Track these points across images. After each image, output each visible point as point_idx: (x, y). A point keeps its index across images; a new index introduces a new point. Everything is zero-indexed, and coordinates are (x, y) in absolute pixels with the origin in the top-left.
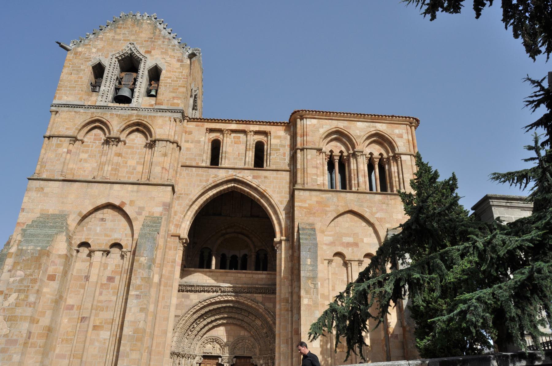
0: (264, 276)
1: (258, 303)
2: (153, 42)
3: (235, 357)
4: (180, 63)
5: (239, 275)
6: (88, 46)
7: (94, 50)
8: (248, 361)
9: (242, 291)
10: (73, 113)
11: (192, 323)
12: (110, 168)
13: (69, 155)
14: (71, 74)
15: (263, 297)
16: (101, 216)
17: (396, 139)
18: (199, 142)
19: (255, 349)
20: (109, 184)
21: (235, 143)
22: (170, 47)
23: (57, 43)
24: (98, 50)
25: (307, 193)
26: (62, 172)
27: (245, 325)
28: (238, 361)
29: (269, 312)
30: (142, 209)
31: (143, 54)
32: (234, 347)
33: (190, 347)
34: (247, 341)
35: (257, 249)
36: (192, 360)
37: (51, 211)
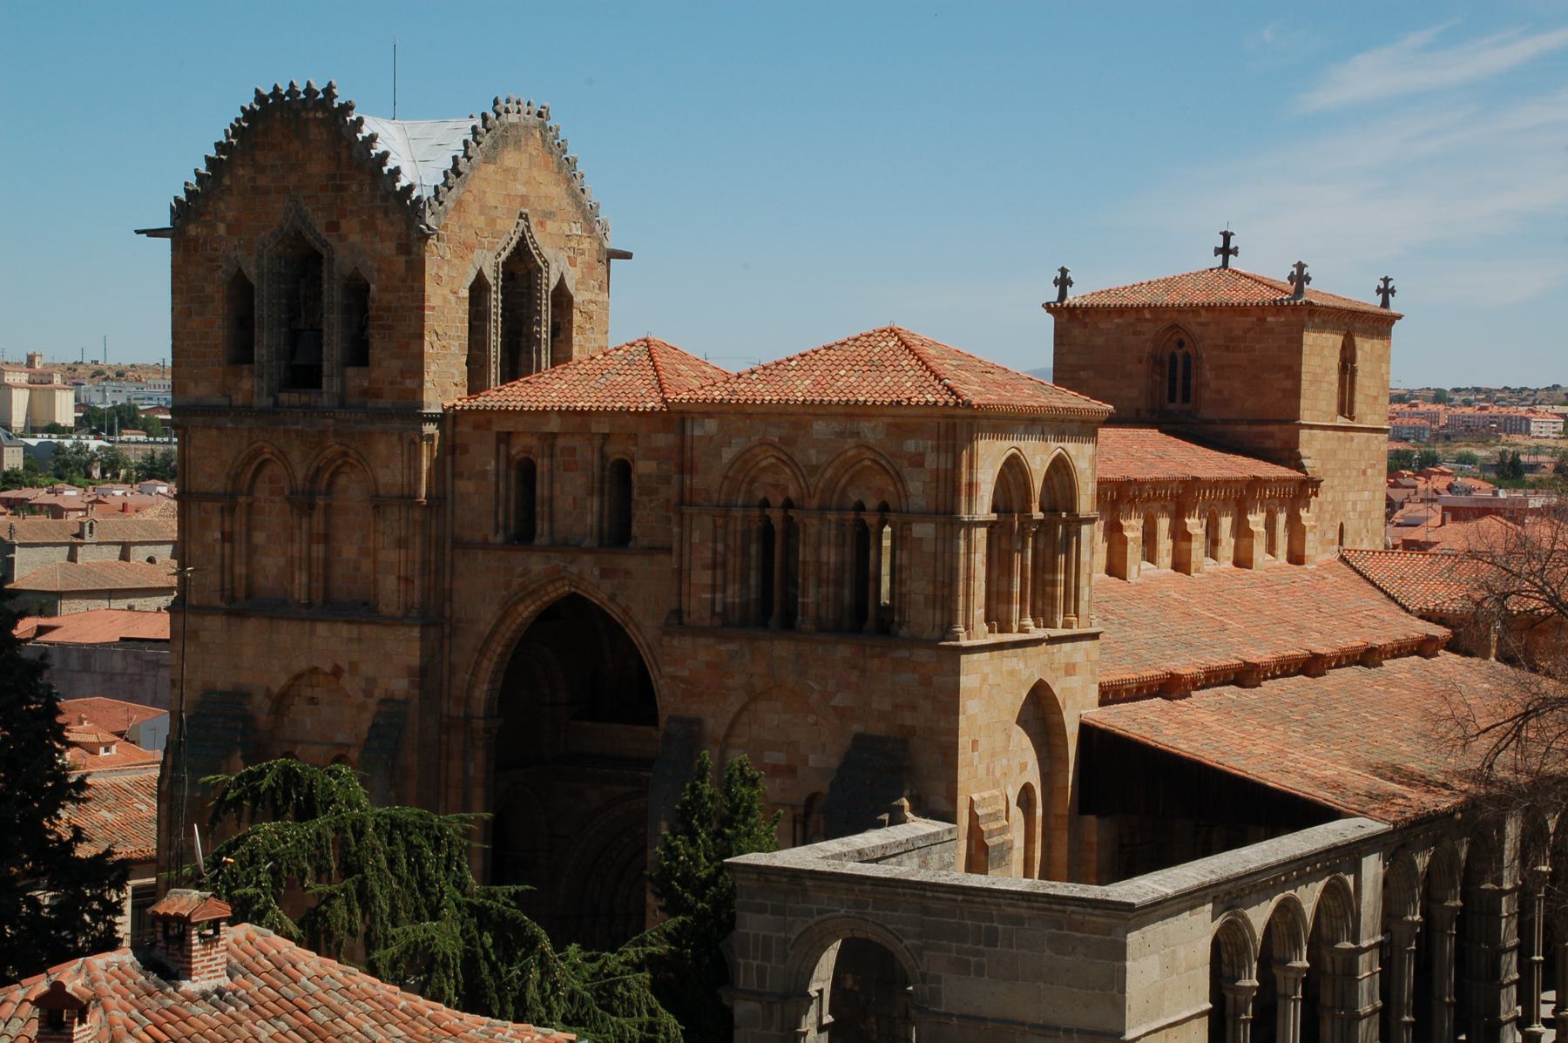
2: (340, 188)
4: (403, 258)
6: (208, 218)
7: (222, 229)
10: (214, 433)
12: (304, 579)
13: (227, 546)
14: (190, 315)
16: (308, 692)
17: (907, 471)
18: (483, 475)
20: (308, 623)
21: (566, 470)
22: (378, 202)
23: (138, 232)
24: (231, 229)
25: (687, 642)
26: (223, 589)
30: (371, 681)
31: (324, 235)
37: (220, 686)
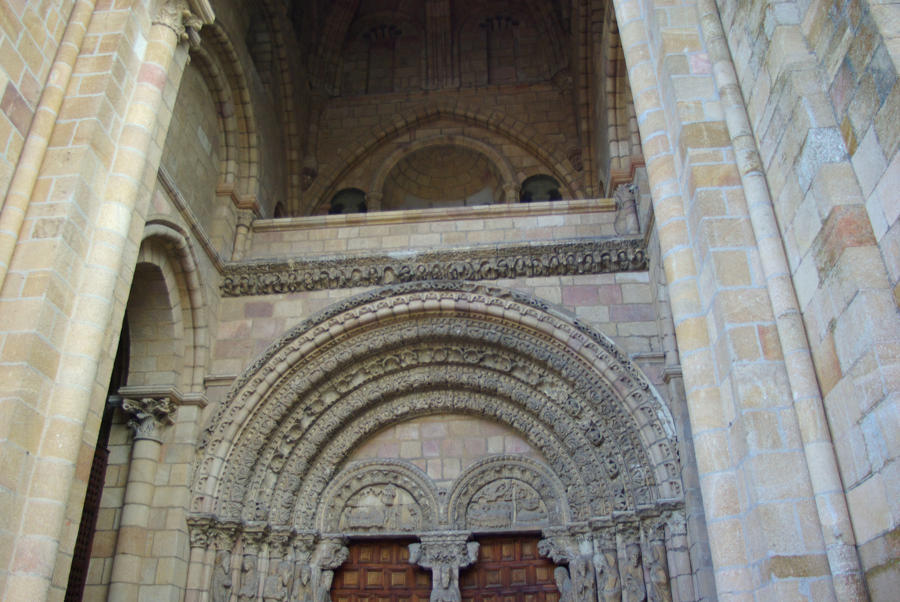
0: (558, 220)
1: (544, 309)
3: (474, 538)
5: (462, 224)
8: (527, 550)
9: (477, 267)
11: (291, 409)
15: (561, 285)
19: (551, 502)
27: (505, 410)
28: (488, 551)
29: (595, 337)
32: (465, 500)
33: (290, 506)
34: (517, 473)
35: (522, 177)
36: (303, 557)
